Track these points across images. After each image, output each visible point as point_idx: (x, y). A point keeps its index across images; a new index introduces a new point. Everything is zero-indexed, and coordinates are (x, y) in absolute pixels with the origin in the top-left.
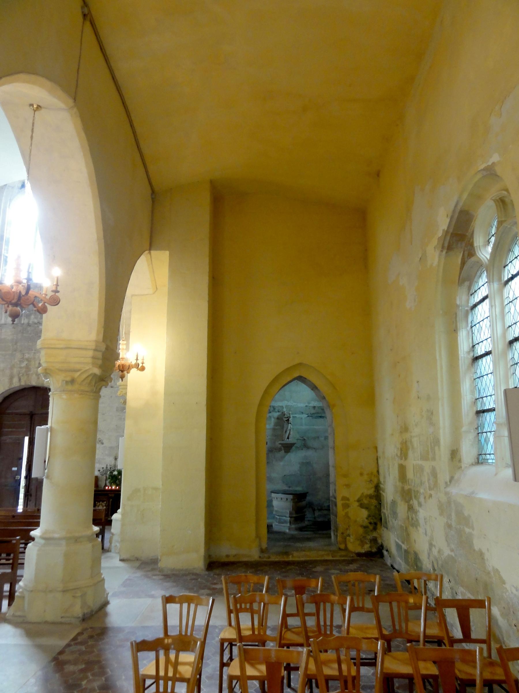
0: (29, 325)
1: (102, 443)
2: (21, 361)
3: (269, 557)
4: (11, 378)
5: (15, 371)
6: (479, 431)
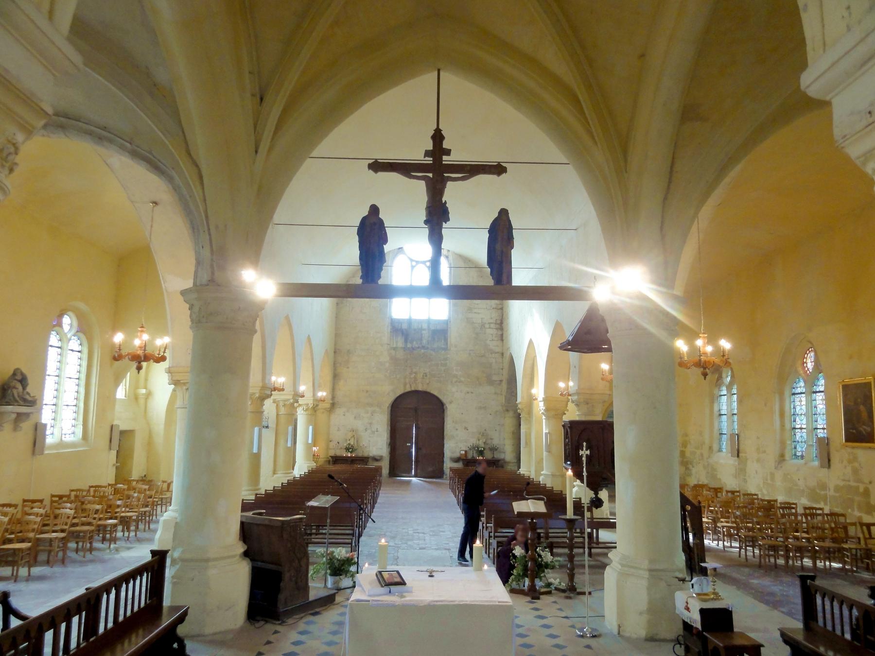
0: (413, 349)
2: (411, 374)
4: (405, 385)
5: (407, 380)
6: (720, 440)
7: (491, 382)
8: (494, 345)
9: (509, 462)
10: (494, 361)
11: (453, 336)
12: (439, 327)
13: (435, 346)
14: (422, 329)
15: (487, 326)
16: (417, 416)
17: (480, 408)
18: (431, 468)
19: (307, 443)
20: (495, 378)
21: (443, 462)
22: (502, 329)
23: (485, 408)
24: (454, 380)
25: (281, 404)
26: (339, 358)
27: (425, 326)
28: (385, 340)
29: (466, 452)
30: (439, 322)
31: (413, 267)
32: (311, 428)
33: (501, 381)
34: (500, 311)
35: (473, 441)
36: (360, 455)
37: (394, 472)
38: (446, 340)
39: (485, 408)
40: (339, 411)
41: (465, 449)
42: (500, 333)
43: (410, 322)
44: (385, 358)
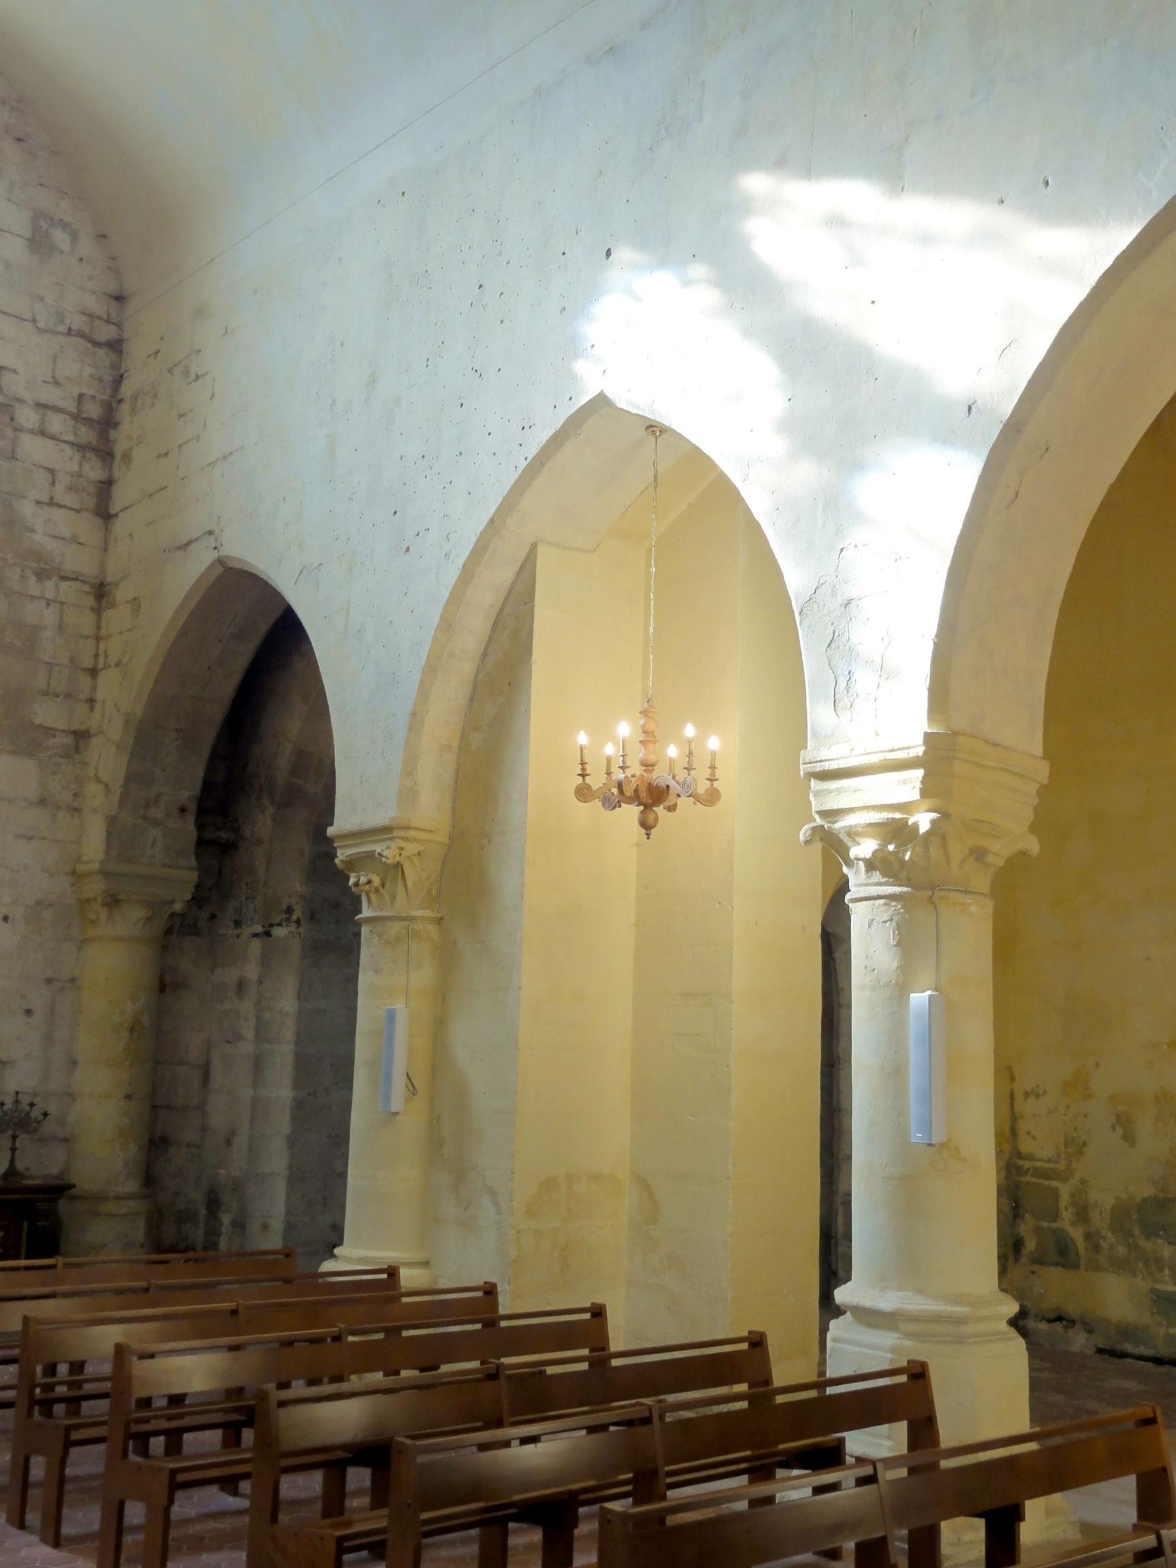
9: (100, 1198)
10: (49, 617)
15: (27, 416)
20: (47, 714)
22: (105, 453)
33: (81, 737)
42: (94, 471)
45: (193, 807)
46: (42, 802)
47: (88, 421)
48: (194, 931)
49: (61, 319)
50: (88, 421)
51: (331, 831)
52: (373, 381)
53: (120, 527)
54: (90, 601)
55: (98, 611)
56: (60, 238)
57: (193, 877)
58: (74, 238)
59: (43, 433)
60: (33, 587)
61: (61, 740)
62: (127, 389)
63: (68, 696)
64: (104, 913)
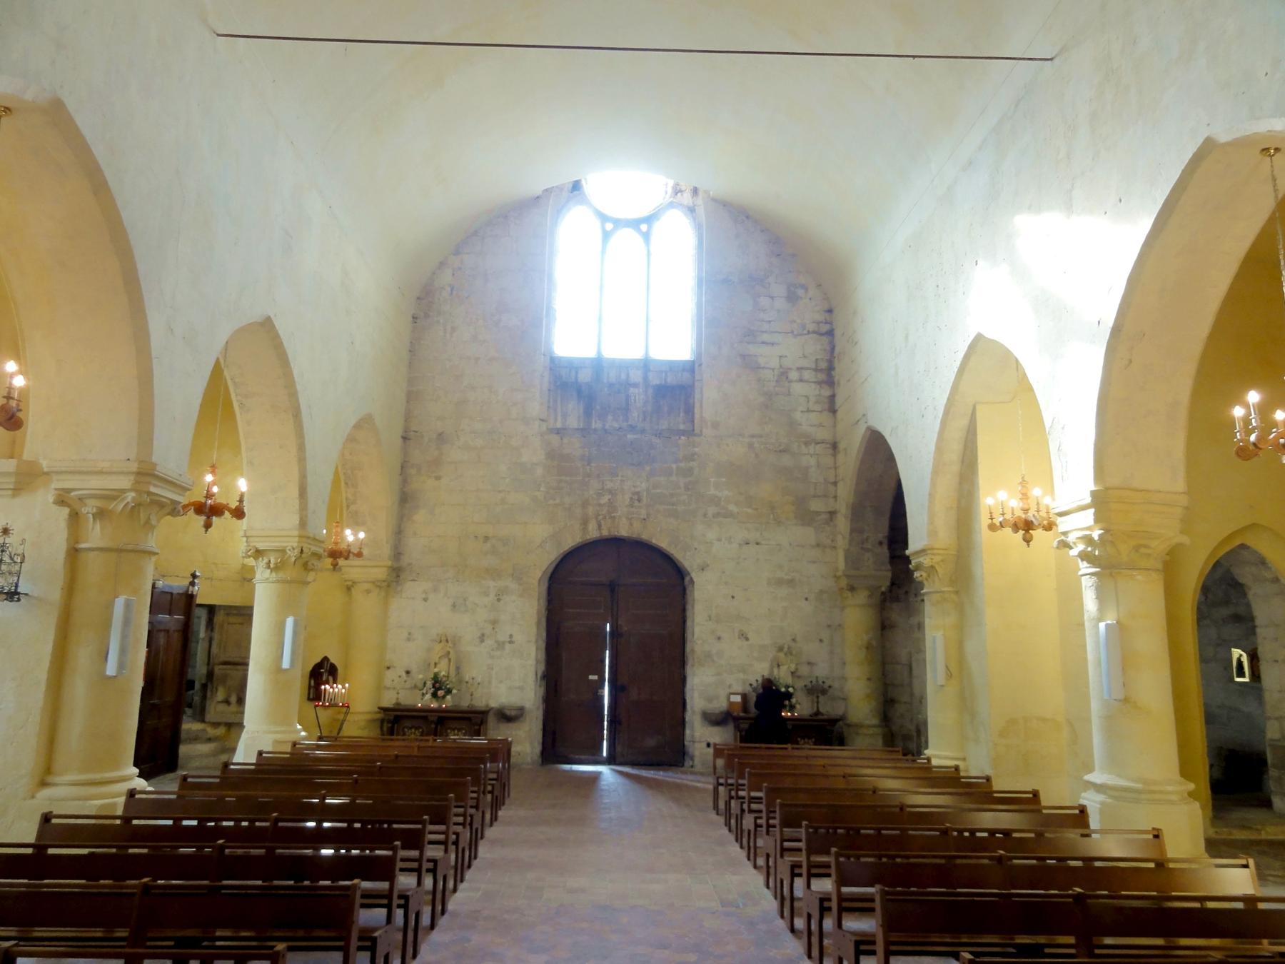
1: (747, 639)
3: (1231, 834)
4: (585, 522)
7: (805, 517)
8: (811, 422)
9: (859, 726)
10: (813, 461)
11: (709, 399)
12: (671, 380)
13: (664, 425)
14: (629, 384)
15: (794, 375)
16: (614, 606)
17: (780, 582)
18: (652, 740)
19: (278, 670)
20: (816, 505)
21: (683, 723)
23: (791, 582)
24: (712, 510)
25: (89, 509)
26: (411, 445)
27: (636, 376)
28: (536, 408)
29: (744, 696)
30: (672, 366)
31: (606, 235)
32: (290, 622)
33: (832, 514)
34: (825, 339)
35: (760, 670)
36: (465, 704)
37: (556, 747)
38: (689, 411)
39: (791, 582)
40: (413, 589)
41: (740, 689)
42: (826, 392)
43: (598, 364)
44: (534, 454)
45: (886, 541)
46: (818, 545)
47: (821, 370)
48: (897, 599)
49: (804, 327)
50: (821, 370)
51: (907, 552)
52: (907, 337)
53: (840, 414)
54: (831, 451)
55: (834, 455)
56: (800, 292)
57: (889, 574)
58: (806, 289)
59: (801, 380)
60: (804, 449)
61: (824, 516)
62: (836, 353)
63: (825, 496)
64: (849, 594)
